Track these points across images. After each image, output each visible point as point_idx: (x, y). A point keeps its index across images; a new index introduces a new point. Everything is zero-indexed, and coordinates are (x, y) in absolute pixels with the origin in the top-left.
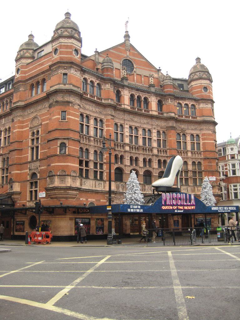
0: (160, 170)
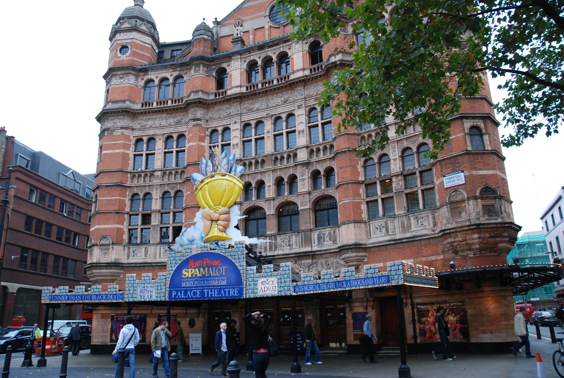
0: (316, 194)
